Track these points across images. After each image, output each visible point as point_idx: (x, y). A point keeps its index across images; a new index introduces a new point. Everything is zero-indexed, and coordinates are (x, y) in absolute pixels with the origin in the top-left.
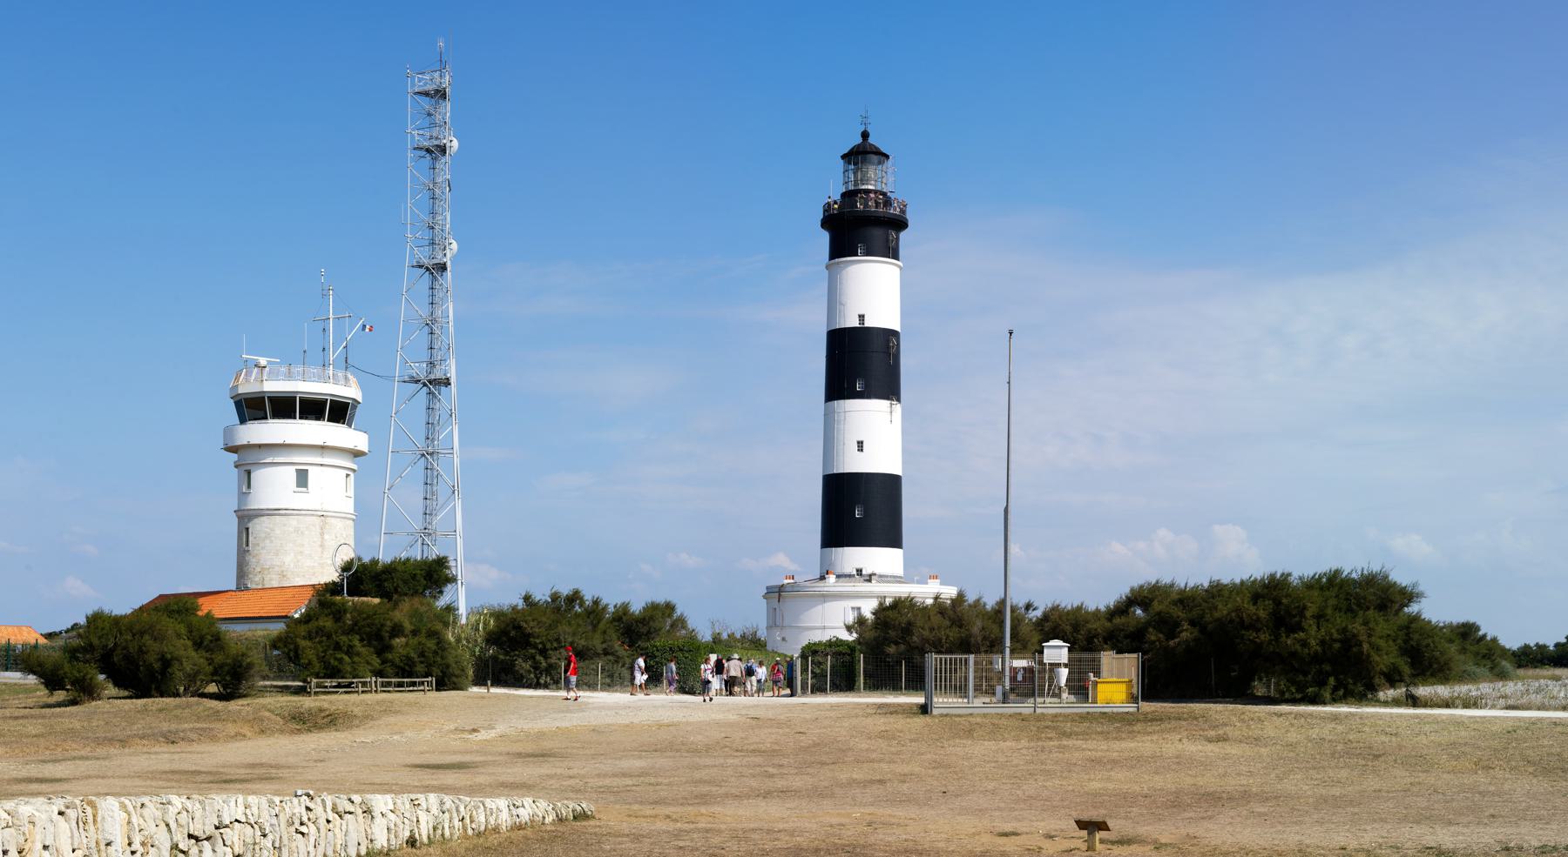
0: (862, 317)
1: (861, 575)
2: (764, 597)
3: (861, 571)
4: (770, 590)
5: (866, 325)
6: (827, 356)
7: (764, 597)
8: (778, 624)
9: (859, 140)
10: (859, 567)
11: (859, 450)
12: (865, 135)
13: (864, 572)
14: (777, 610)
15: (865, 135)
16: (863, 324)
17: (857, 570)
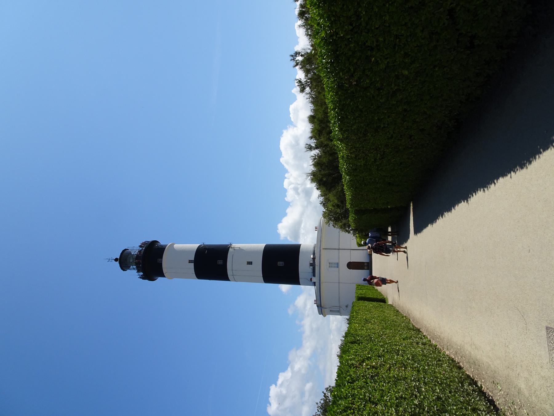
0: (190, 262)
1: (313, 264)
2: (325, 316)
3: (311, 264)
4: (321, 313)
5: (193, 259)
6: (210, 280)
7: (325, 316)
8: (338, 310)
9: (118, 262)
10: (308, 265)
11: (252, 264)
12: (116, 260)
13: (312, 262)
14: (331, 309)
15: (116, 260)
16: (193, 261)
17: (311, 266)
